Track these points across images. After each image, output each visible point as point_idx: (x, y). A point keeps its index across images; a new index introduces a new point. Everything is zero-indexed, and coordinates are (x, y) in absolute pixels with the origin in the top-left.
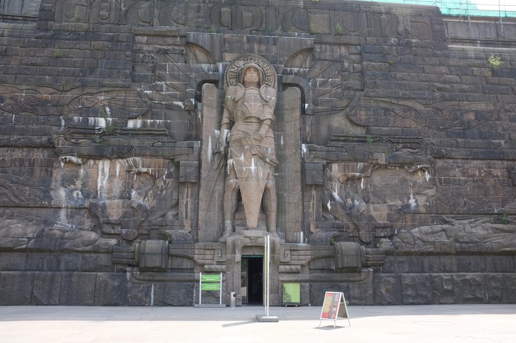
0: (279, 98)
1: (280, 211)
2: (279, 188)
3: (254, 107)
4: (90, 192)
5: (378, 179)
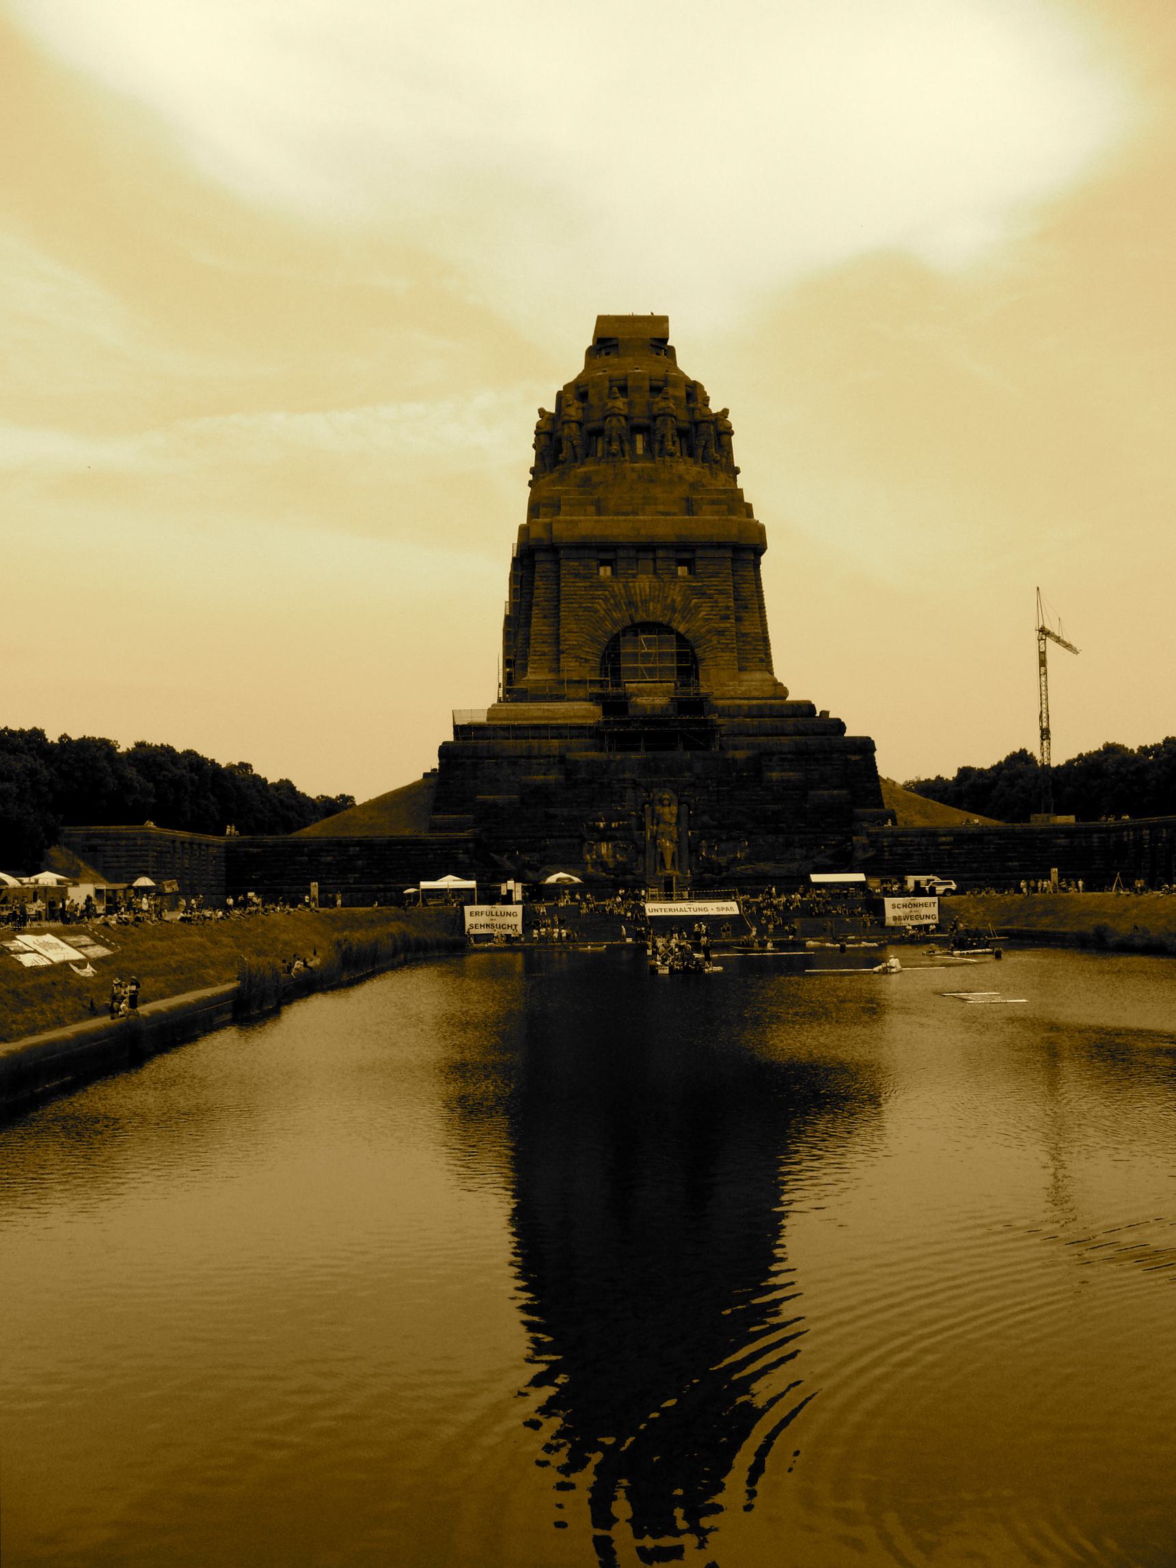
0: (679, 810)
1: (680, 861)
2: (679, 851)
3: (668, 817)
4: (599, 856)
5: (723, 846)
